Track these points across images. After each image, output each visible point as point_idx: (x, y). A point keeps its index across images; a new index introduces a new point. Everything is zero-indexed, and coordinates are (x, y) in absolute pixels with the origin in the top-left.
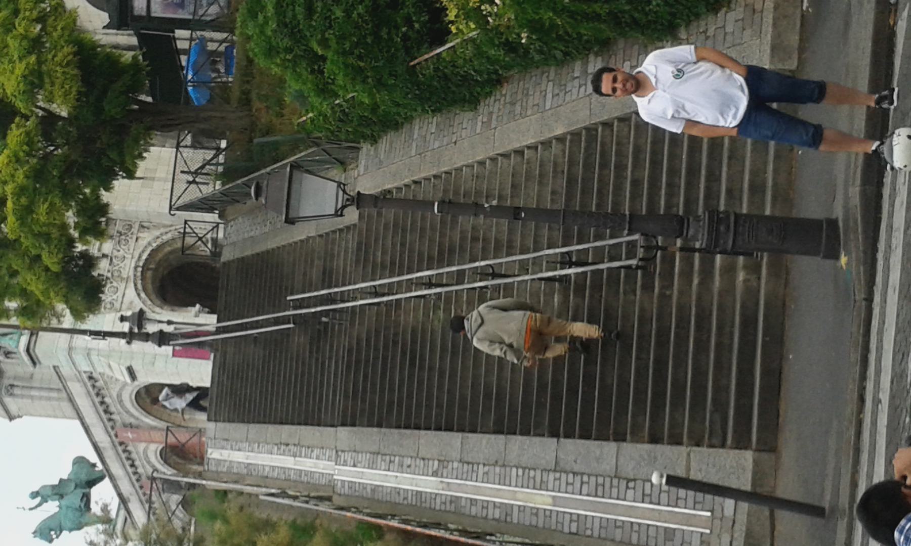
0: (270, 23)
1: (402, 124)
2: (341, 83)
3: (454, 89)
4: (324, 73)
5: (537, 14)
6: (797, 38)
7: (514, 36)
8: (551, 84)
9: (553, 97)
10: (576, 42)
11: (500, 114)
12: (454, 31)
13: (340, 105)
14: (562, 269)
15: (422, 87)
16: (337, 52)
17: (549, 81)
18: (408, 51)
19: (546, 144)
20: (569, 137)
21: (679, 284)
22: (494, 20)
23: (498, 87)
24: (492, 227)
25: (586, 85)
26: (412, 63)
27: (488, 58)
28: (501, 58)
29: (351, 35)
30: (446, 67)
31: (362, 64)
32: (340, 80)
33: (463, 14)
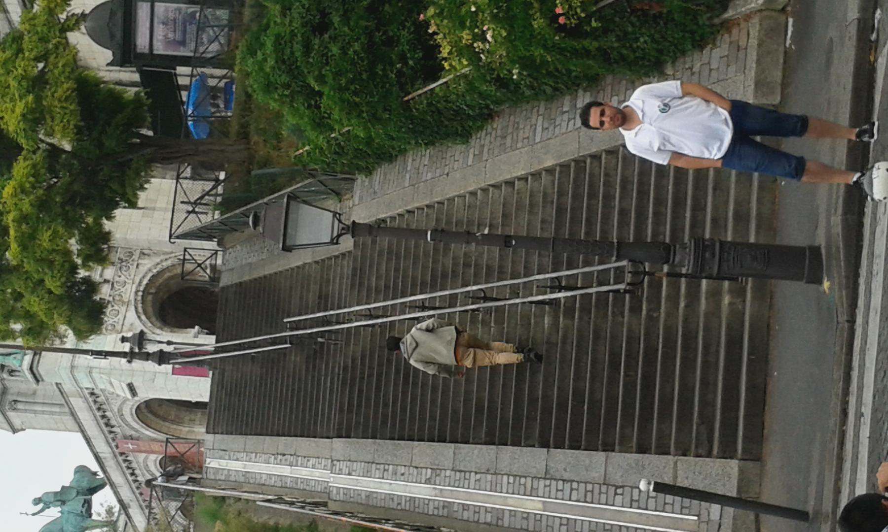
0: (269, 60)
1: (396, 156)
2: (337, 117)
3: (447, 123)
4: (320, 107)
5: (529, 51)
6: (780, 74)
7: (506, 72)
8: (540, 118)
9: (543, 130)
10: (565, 78)
11: (491, 147)
12: (447, 68)
13: (336, 139)
14: (551, 293)
15: (416, 121)
16: (333, 88)
17: (538, 115)
18: (402, 87)
19: (536, 175)
20: (558, 169)
21: (666, 307)
22: (487, 57)
23: (490, 121)
24: (483, 253)
25: (574, 118)
26: (406, 99)
27: (480, 94)
28: (493, 93)
29: (347, 71)
30: (439, 102)
31: (357, 100)
32: (336, 116)
33: (456, 51)
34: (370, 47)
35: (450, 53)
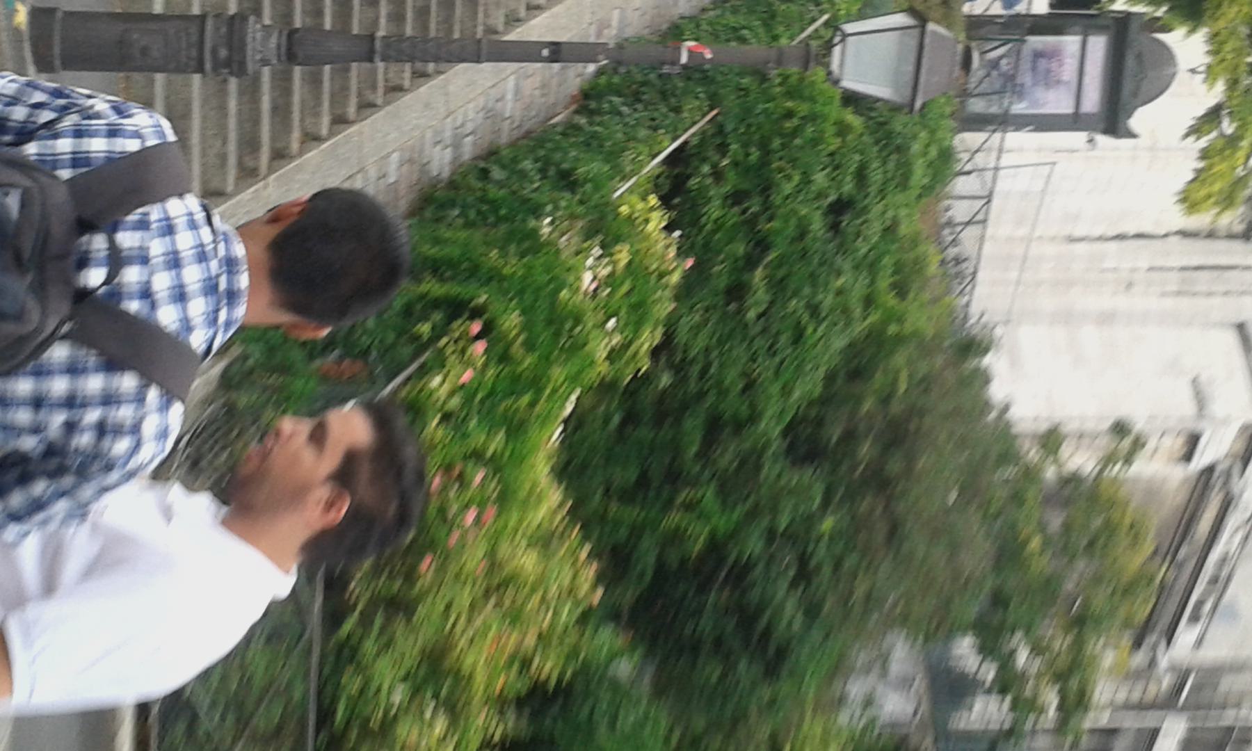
16: (825, 118)
26: (714, 112)
29: (802, 148)
34: (766, 189)
35: (647, 221)
